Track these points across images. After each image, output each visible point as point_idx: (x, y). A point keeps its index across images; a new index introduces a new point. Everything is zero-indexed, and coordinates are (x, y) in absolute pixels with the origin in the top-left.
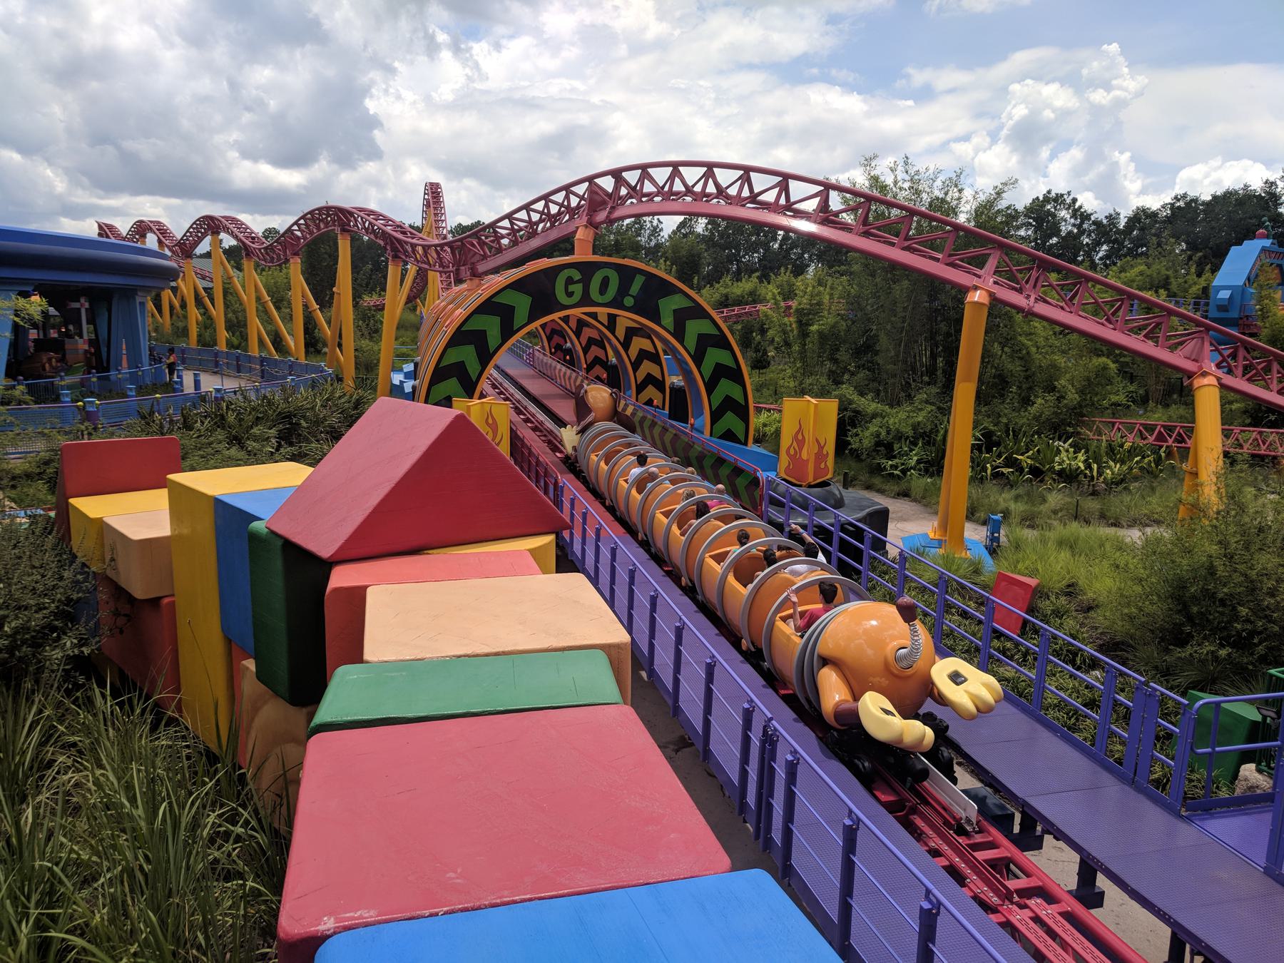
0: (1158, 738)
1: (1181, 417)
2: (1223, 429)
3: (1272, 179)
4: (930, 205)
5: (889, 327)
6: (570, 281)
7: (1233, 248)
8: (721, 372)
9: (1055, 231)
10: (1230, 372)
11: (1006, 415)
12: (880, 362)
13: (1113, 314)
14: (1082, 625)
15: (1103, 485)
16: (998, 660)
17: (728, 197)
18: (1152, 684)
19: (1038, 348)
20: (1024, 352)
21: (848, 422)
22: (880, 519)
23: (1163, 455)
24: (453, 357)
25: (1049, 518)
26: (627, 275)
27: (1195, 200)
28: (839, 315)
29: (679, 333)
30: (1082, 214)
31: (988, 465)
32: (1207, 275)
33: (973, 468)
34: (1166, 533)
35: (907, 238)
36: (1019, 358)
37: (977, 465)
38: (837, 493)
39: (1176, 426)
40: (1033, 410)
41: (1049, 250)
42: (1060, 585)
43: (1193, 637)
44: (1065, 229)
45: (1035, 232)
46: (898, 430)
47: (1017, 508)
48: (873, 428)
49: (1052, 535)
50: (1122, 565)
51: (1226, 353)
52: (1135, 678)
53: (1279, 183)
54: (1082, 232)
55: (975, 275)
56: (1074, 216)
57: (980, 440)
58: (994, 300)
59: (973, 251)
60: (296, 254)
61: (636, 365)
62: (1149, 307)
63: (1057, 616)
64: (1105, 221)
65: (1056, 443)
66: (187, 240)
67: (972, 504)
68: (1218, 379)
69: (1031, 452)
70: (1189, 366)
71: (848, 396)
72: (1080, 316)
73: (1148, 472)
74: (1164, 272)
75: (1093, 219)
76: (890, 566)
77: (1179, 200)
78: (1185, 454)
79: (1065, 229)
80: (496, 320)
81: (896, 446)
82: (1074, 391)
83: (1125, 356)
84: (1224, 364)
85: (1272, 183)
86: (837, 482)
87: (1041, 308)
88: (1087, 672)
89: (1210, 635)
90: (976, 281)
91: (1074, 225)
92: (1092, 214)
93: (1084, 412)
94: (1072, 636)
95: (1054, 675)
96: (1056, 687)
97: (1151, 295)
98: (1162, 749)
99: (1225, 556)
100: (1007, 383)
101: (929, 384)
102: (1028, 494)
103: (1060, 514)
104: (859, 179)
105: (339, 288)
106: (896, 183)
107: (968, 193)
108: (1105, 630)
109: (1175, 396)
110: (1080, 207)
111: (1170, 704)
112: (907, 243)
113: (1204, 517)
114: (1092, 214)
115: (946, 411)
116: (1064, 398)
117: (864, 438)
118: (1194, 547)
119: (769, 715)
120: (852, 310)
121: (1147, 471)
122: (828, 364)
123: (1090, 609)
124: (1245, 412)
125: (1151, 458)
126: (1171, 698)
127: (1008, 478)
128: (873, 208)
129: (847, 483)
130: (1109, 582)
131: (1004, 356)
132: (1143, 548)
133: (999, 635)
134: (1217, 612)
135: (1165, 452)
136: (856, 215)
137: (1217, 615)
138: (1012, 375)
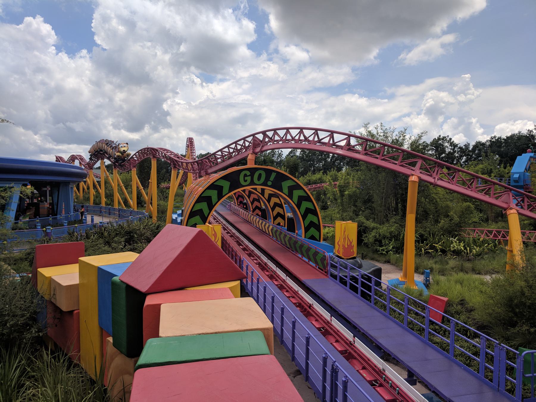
0: (507, 369)
1: (503, 227)
2: (521, 232)
3: (531, 129)
4: (392, 142)
5: (377, 191)
6: (245, 175)
7: (518, 157)
8: (308, 211)
9: (444, 151)
10: (522, 208)
11: (428, 227)
13: (471, 184)
14: (469, 318)
15: (472, 256)
16: (433, 334)
17: (309, 141)
18: (502, 344)
20: (435, 201)
21: (362, 232)
22: (378, 273)
23: (497, 243)
24: (198, 207)
25: (451, 271)
26: (269, 172)
27: (500, 138)
28: (356, 187)
29: (290, 195)
31: (423, 249)
32: (508, 168)
33: (416, 250)
35: (383, 156)
37: (418, 249)
38: (359, 261)
39: (502, 231)
40: (440, 225)
41: (442, 159)
43: (518, 323)
44: (448, 150)
46: (384, 235)
47: (436, 267)
48: (373, 234)
49: (452, 278)
51: (519, 200)
52: (494, 342)
53: (533, 131)
55: (412, 170)
56: (451, 145)
57: (418, 238)
58: (420, 180)
61: (273, 209)
62: (486, 181)
63: (457, 314)
64: (464, 147)
65: (451, 239)
68: (517, 211)
69: (440, 243)
70: (505, 205)
73: (491, 250)
74: (489, 167)
77: (493, 139)
78: (506, 243)
79: (448, 150)
80: (215, 192)
81: (383, 241)
82: (457, 217)
83: (477, 202)
84: (519, 204)
85: (531, 131)
86: (359, 257)
87: (440, 183)
88: (472, 339)
89: (526, 322)
90: (413, 172)
91: (451, 149)
93: (462, 225)
94: (464, 323)
95: (459, 341)
96: (460, 346)
98: (510, 375)
100: (428, 214)
101: (395, 215)
102: (441, 261)
103: (455, 270)
105: (151, 180)
106: (378, 133)
107: (407, 137)
108: (479, 320)
109: (500, 218)
110: (453, 142)
111: (511, 354)
112: (383, 158)
113: (517, 269)
114: (458, 144)
115: (403, 226)
116: (453, 220)
117: (370, 238)
118: (514, 283)
119: (334, 360)
123: (471, 310)
124: (530, 224)
125: (492, 245)
126: (511, 351)
127: (431, 254)
128: (369, 143)
129: (364, 257)
131: (426, 203)
132: (492, 284)
133: (432, 323)
134: (528, 311)
135: (498, 242)
136: (362, 147)
137: (528, 313)
138: (430, 211)
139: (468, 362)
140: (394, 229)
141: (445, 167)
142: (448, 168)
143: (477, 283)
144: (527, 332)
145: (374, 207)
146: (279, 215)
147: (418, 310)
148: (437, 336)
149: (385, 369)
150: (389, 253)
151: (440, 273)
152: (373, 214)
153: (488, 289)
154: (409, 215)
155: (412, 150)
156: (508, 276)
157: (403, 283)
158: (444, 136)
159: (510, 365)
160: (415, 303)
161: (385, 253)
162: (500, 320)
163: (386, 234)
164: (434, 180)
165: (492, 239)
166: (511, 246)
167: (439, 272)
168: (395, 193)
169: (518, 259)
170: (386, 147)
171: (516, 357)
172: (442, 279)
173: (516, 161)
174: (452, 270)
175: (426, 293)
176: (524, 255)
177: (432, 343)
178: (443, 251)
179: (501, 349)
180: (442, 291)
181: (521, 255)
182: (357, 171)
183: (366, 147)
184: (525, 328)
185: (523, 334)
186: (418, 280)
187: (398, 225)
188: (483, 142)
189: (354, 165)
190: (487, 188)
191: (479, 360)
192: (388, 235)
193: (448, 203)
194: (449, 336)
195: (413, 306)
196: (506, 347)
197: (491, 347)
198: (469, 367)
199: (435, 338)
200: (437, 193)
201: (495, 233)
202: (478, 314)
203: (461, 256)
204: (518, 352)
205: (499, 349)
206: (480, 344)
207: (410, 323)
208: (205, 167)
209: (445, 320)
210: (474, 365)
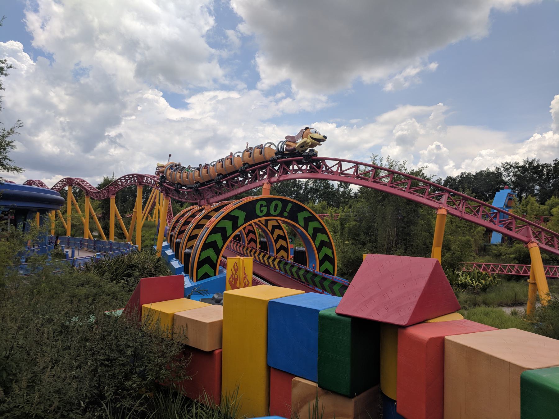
3: (498, 167)
6: (262, 206)
7: (497, 193)
8: (323, 244)
26: (285, 203)
29: (306, 227)
53: (501, 168)
60: (114, 195)
61: (276, 241)
66: (55, 188)
85: (499, 168)
105: (136, 209)
124: (515, 258)
146: (282, 248)
154: (436, 248)
188: (454, 177)
201: (484, 267)
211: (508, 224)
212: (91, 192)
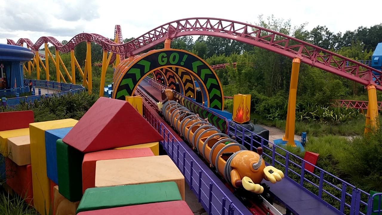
0: (361, 207)
1: (364, 99)
2: (378, 103)
4: (280, 30)
5: (267, 71)
6: (163, 57)
8: (213, 86)
9: (321, 39)
10: (379, 84)
11: (306, 99)
12: (265, 82)
13: (341, 66)
14: (334, 169)
15: (339, 122)
16: (307, 181)
18: (358, 189)
19: (316, 77)
20: (312, 78)
21: (254, 102)
22: (266, 135)
23: (358, 111)
25: (322, 133)
26: (182, 54)
27: (365, 28)
28: (251, 67)
29: (199, 74)
30: (329, 33)
31: (301, 116)
32: (371, 52)
33: (296, 117)
34: (361, 138)
35: (273, 42)
36: (310, 80)
37: (298, 116)
38: (252, 126)
39: (362, 102)
40: (315, 97)
41: (319, 45)
42: (326, 155)
43: (371, 172)
44: (324, 38)
45: (314, 39)
46: (272, 105)
47: (311, 130)
48: (263, 104)
49: (323, 139)
50: (346, 149)
51: (378, 78)
52: (352, 187)
54: (329, 39)
55: (295, 53)
56: (327, 34)
57: (298, 107)
58: (302, 61)
59: (296, 45)
60: (73, 49)
61: (185, 84)
62: (353, 62)
63: (326, 166)
64: (337, 35)
65: (323, 108)
67: (297, 129)
68: (375, 86)
69: (315, 111)
70: (366, 82)
71: (255, 94)
72: (330, 66)
73: (354, 117)
74: (356, 52)
75: (333, 35)
76: (270, 150)
77: (360, 29)
78: (366, 111)
79: (324, 38)
80: (139, 70)
81: (271, 110)
82: (329, 91)
83: (345, 79)
84: (377, 82)
86: (252, 122)
87: (317, 64)
88: (336, 185)
89: (377, 172)
90: (296, 56)
91: (327, 37)
92: (332, 33)
93: (332, 98)
94: (331, 173)
95: (326, 186)
96: (326, 190)
97: (353, 59)
98: (362, 210)
99: (380, 145)
100: (307, 89)
101: (281, 89)
102: (315, 125)
103: (325, 132)
104: (256, 22)
106: (269, 24)
107: (292, 27)
108: (342, 171)
109: (362, 92)
110: (329, 31)
111: (364, 195)
112: (273, 43)
113: (373, 132)
114: (332, 33)
115: (287, 98)
116: (325, 93)
117: (260, 107)
118: (370, 142)
119: (231, 202)
120: (255, 65)
121: (353, 117)
122: (248, 83)
123: (336, 163)
125: (355, 113)
126: (364, 193)
127: (308, 120)
128: (262, 32)
129: (255, 122)
130: (342, 154)
131: (305, 80)
132: (353, 143)
133: (306, 173)
134: (379, 164)
135: (359, 111)
136: (256, 34)
137: (378, 165)
138: (308, 86)
139: (332, 202)
140: (280, 100)
141: (321, 51)
142: (324, 52)
143: (341, 142)
144: (377, 179)
145: (264, 83)
147: (296, 163)
148: (310, 183)
149: (270, 208)
150: (275, 119)
151: (314, 135)
152: (263, 88)
153: (349, 147)
154: (292, 89)
155: (296, 38)
156: (366, 137)
157: (284, 142)
158: (321, 26)
159: (363, 204)
160: (294, 158)
161: (272, 119)
162: (358, 171)
163: (273, 105)
164: (312, 62)
165: (355, 108)
166: (369, 114)
167: (313, 134)
168: (282, 72)
169: (374, 124)
170: (275, 35)
171: (368, 198)
172: (316, 139)
173: (377, 47)
174: (323, 133)
175: (303, 150)
176: (379, 121)
177: (306, 188)
178: (317, 118)
179: (357, 192)
180: (315, 148)
181: (376, 121)
182: (252, 54)
183: (260, 34)
184: (376, 176)
185: (374, 180)
186: (296, 140)
187: (283, 97)
189: (249, 49)
190: (353, 69)
191: (340, 200)
192: (275, 105)
193: (322, 80)
194: (319, 182)
195: (292, 160)
196: (361, 191)
197: (350, 190)
198: (332, 205)
199: (308, 184)
200: (314, 72)
202: (341, 166)
203: (330, 122)
204: (370, 195)
205: (356, 192)
206: (341, 189)
207: (290, 173)
208: (130, 49)
209: (316, 170)
210: (336, 204)
211: (354, 70)
212: (59, 47)
